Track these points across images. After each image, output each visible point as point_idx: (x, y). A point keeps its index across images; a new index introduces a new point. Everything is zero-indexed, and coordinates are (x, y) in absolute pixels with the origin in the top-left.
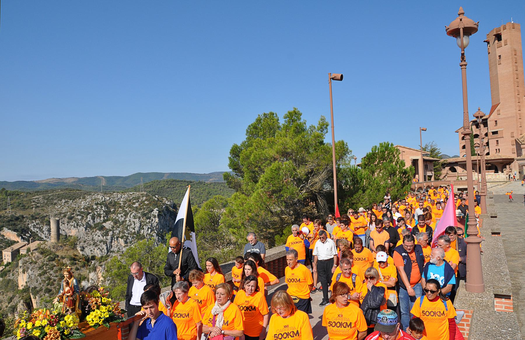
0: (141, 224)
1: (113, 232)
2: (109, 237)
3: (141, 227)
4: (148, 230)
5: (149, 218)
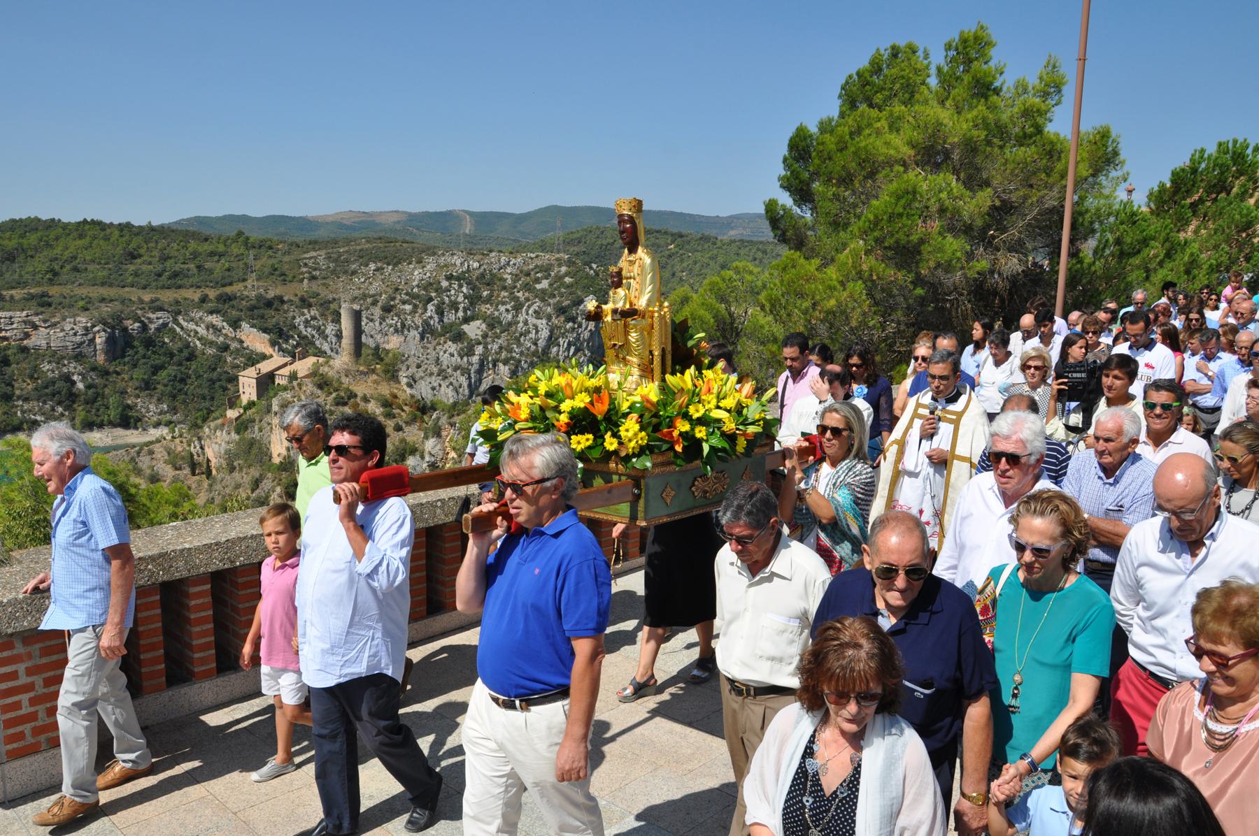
0: (551, 331)
1: (486, 347)
2: (475, 359)
3: (552, 341)
4: (568, 349)
5: (573, 320)
